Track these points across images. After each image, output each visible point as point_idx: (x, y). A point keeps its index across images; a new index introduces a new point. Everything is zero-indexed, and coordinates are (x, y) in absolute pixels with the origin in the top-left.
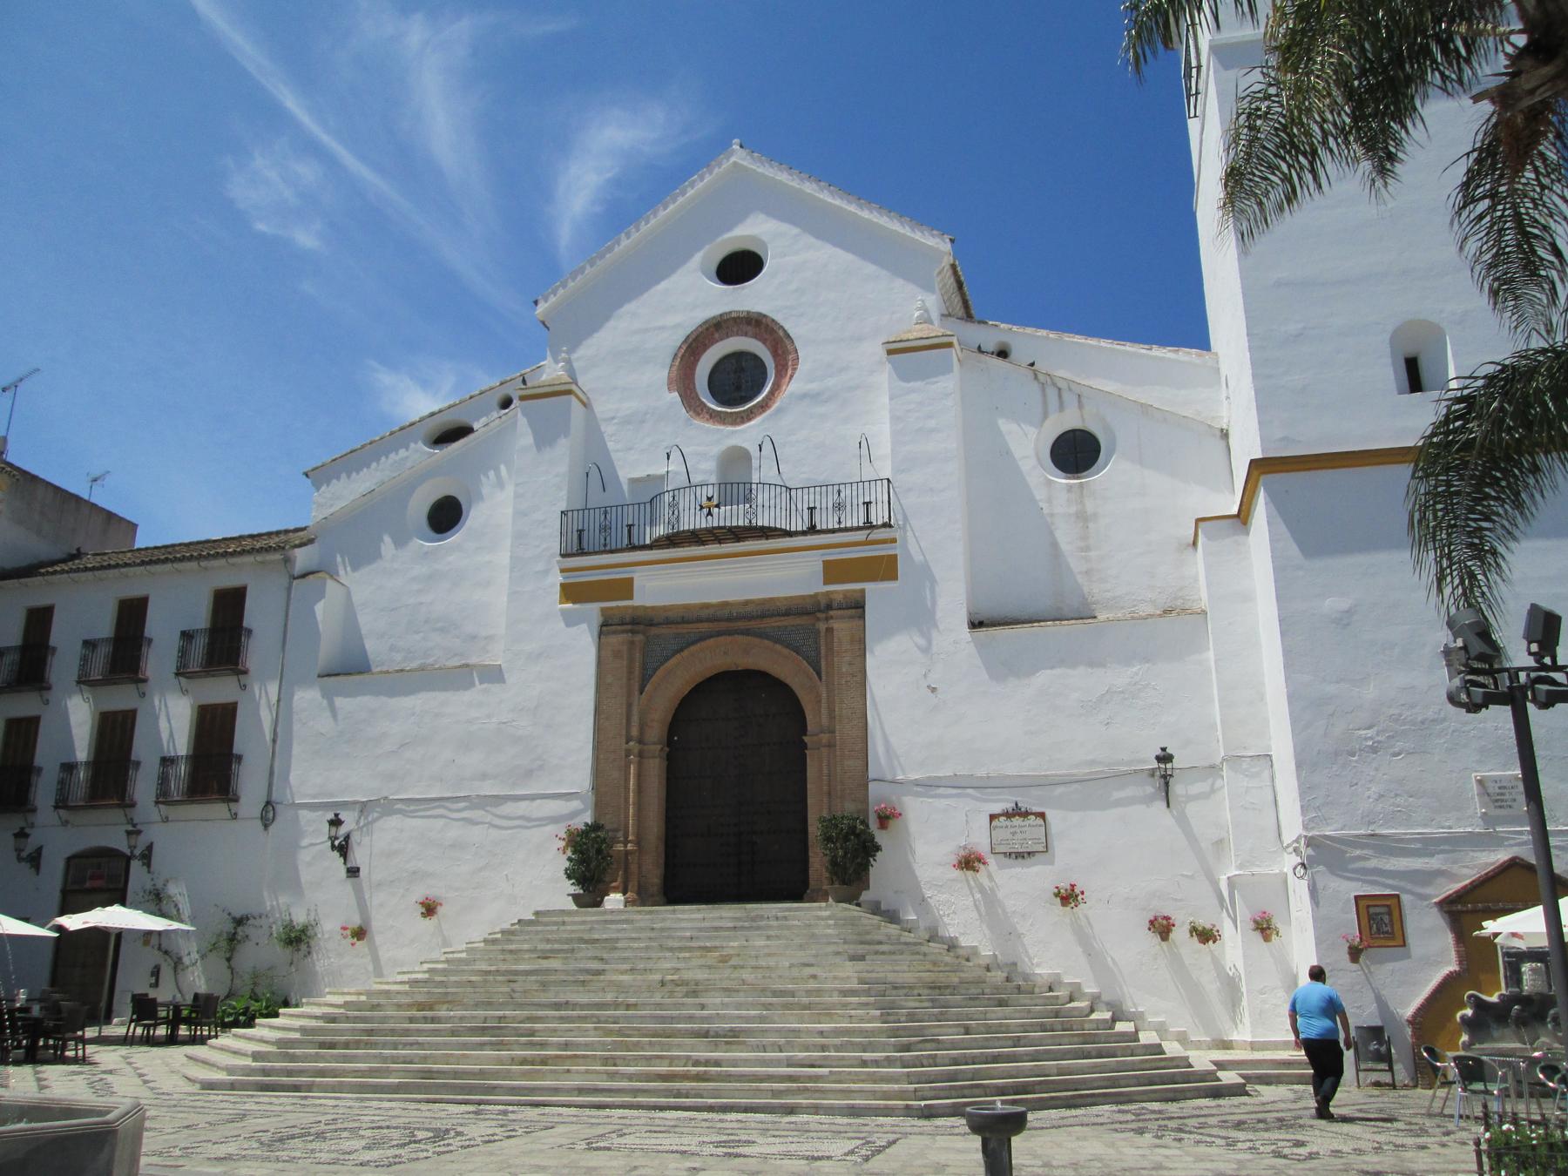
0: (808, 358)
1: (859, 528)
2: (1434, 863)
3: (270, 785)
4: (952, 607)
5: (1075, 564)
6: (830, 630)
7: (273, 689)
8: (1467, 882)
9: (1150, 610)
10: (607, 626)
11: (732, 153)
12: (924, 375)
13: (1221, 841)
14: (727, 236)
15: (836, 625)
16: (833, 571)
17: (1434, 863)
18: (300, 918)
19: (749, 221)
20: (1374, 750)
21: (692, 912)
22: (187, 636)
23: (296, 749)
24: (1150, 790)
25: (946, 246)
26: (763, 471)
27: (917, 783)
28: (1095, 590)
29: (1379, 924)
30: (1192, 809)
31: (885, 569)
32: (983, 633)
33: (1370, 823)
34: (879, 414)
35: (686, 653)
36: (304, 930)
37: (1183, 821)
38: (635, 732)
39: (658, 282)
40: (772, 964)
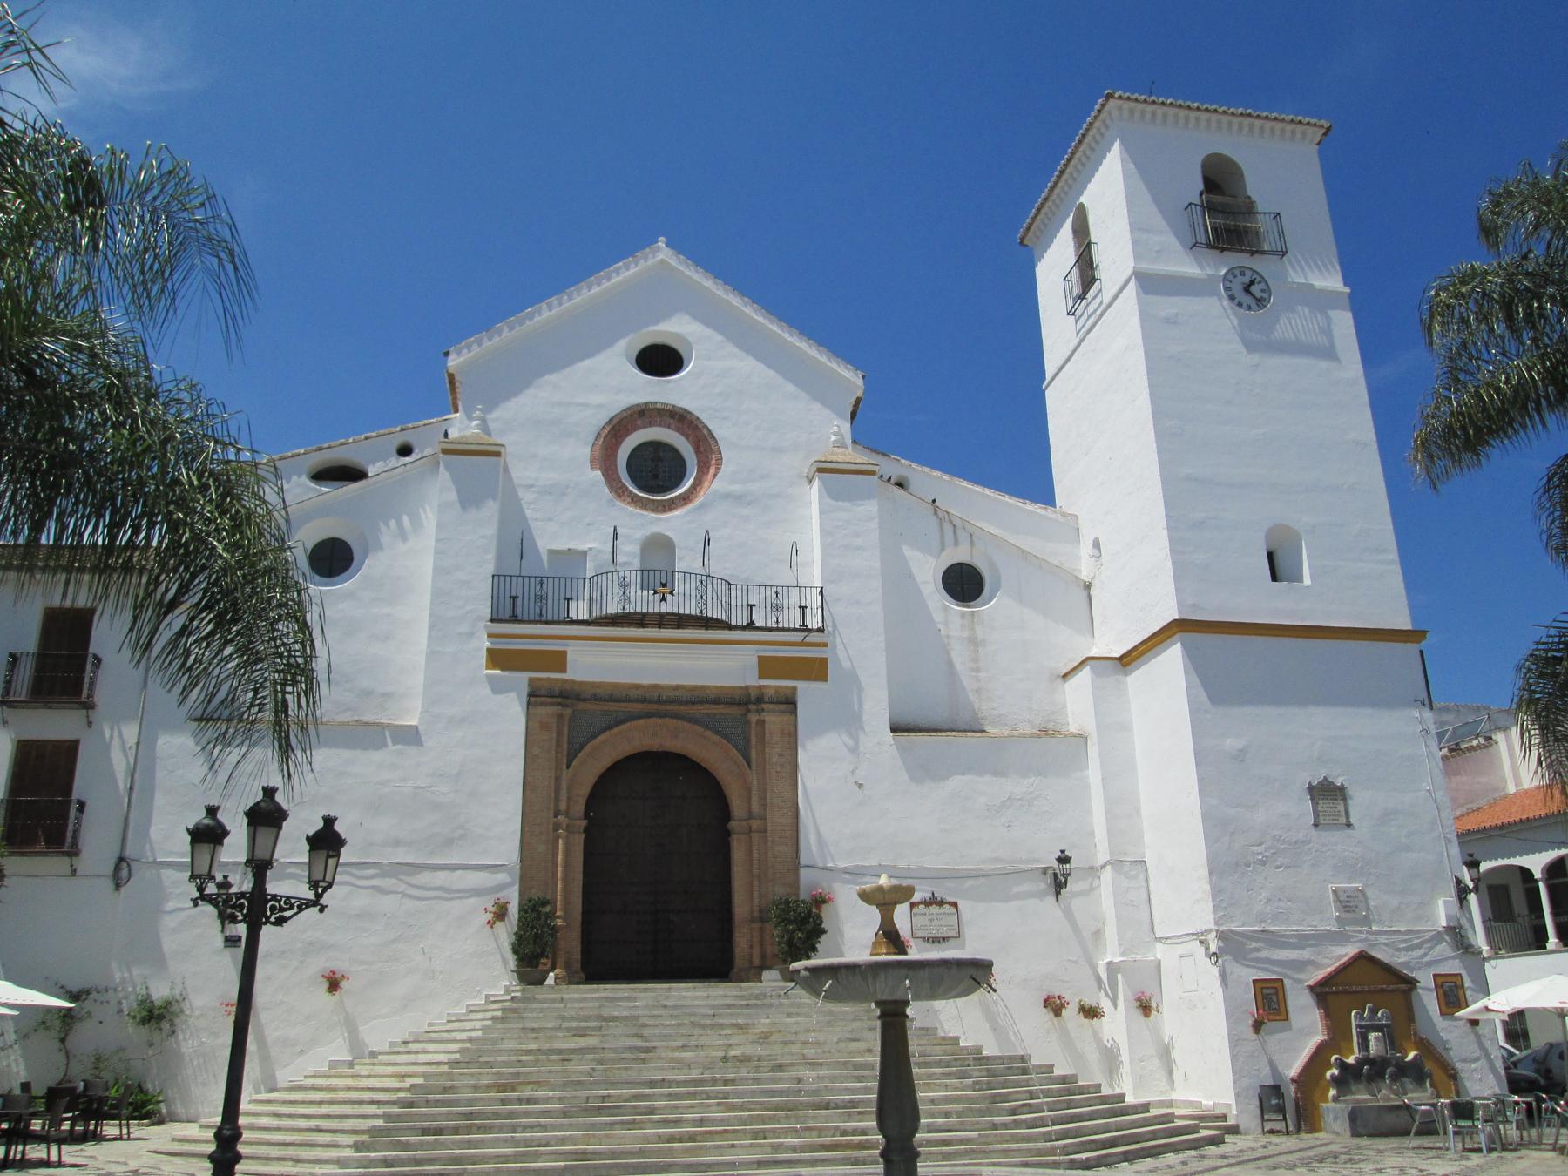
0: (731, 460)
1: (795, 630)
2: (1305, 954)
3: (124, 839)
4: (876, 712)
5: (967, 681)
6: (761, 723)
7: (130, 732)
8: (1330, 970)
9: (1028, 730)
10: (535, 696)
11: (659, 249)
12: (853, 496)
13: (1098, 931)
14: (652, 328)
15: (765, 716)
16: (767, 667)
17: (1305, 954)
18: (160, 991)
19: (674, 319)
20: (1263, 863)
21: (688, 990)
22: (14, 659)
23: (159, 799)
24: (1042, 886)
25: (860, 382)
26: (686, 561)
27: (846, 871)
28: (984, 707)
29: (1269, 1003)
30: (1077, 904)
31: (817, 670)
32: (904, 738)
33: (1262, 921)
34: (793, 523)
35: (615, 730)
36: (168, 1004)
37: (1068, 913)
38: (563, 807)
39: (582, 359)
40: (822, 1039)
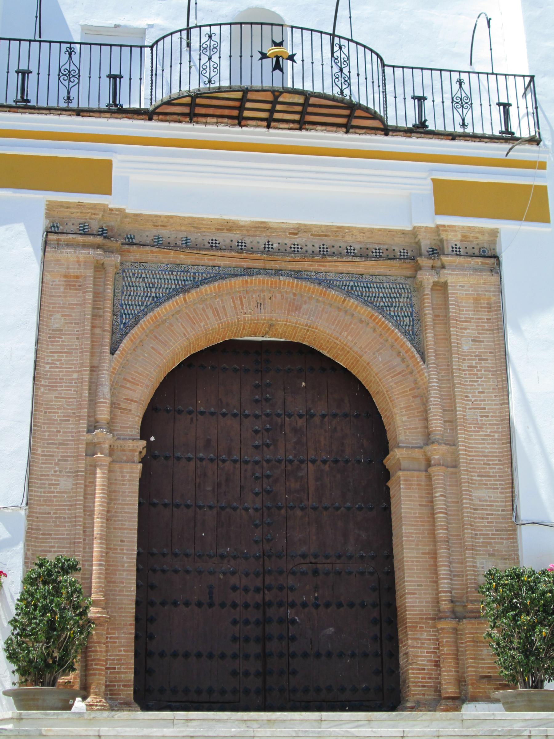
1: (492, 139)
6: (442, 288)
10: (55, 233)
16: (448, 197)
38: (103, 414)
